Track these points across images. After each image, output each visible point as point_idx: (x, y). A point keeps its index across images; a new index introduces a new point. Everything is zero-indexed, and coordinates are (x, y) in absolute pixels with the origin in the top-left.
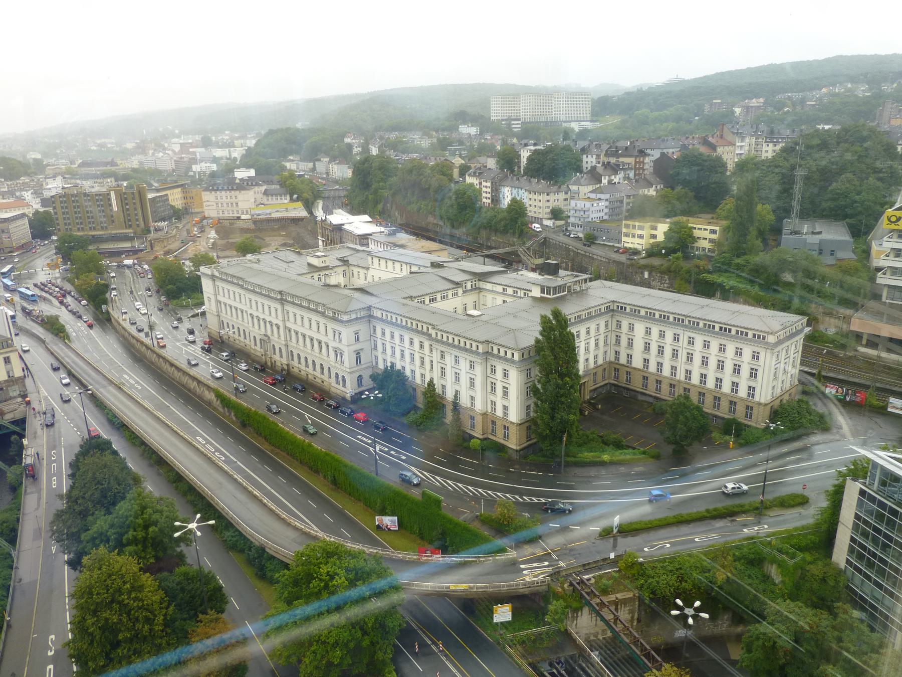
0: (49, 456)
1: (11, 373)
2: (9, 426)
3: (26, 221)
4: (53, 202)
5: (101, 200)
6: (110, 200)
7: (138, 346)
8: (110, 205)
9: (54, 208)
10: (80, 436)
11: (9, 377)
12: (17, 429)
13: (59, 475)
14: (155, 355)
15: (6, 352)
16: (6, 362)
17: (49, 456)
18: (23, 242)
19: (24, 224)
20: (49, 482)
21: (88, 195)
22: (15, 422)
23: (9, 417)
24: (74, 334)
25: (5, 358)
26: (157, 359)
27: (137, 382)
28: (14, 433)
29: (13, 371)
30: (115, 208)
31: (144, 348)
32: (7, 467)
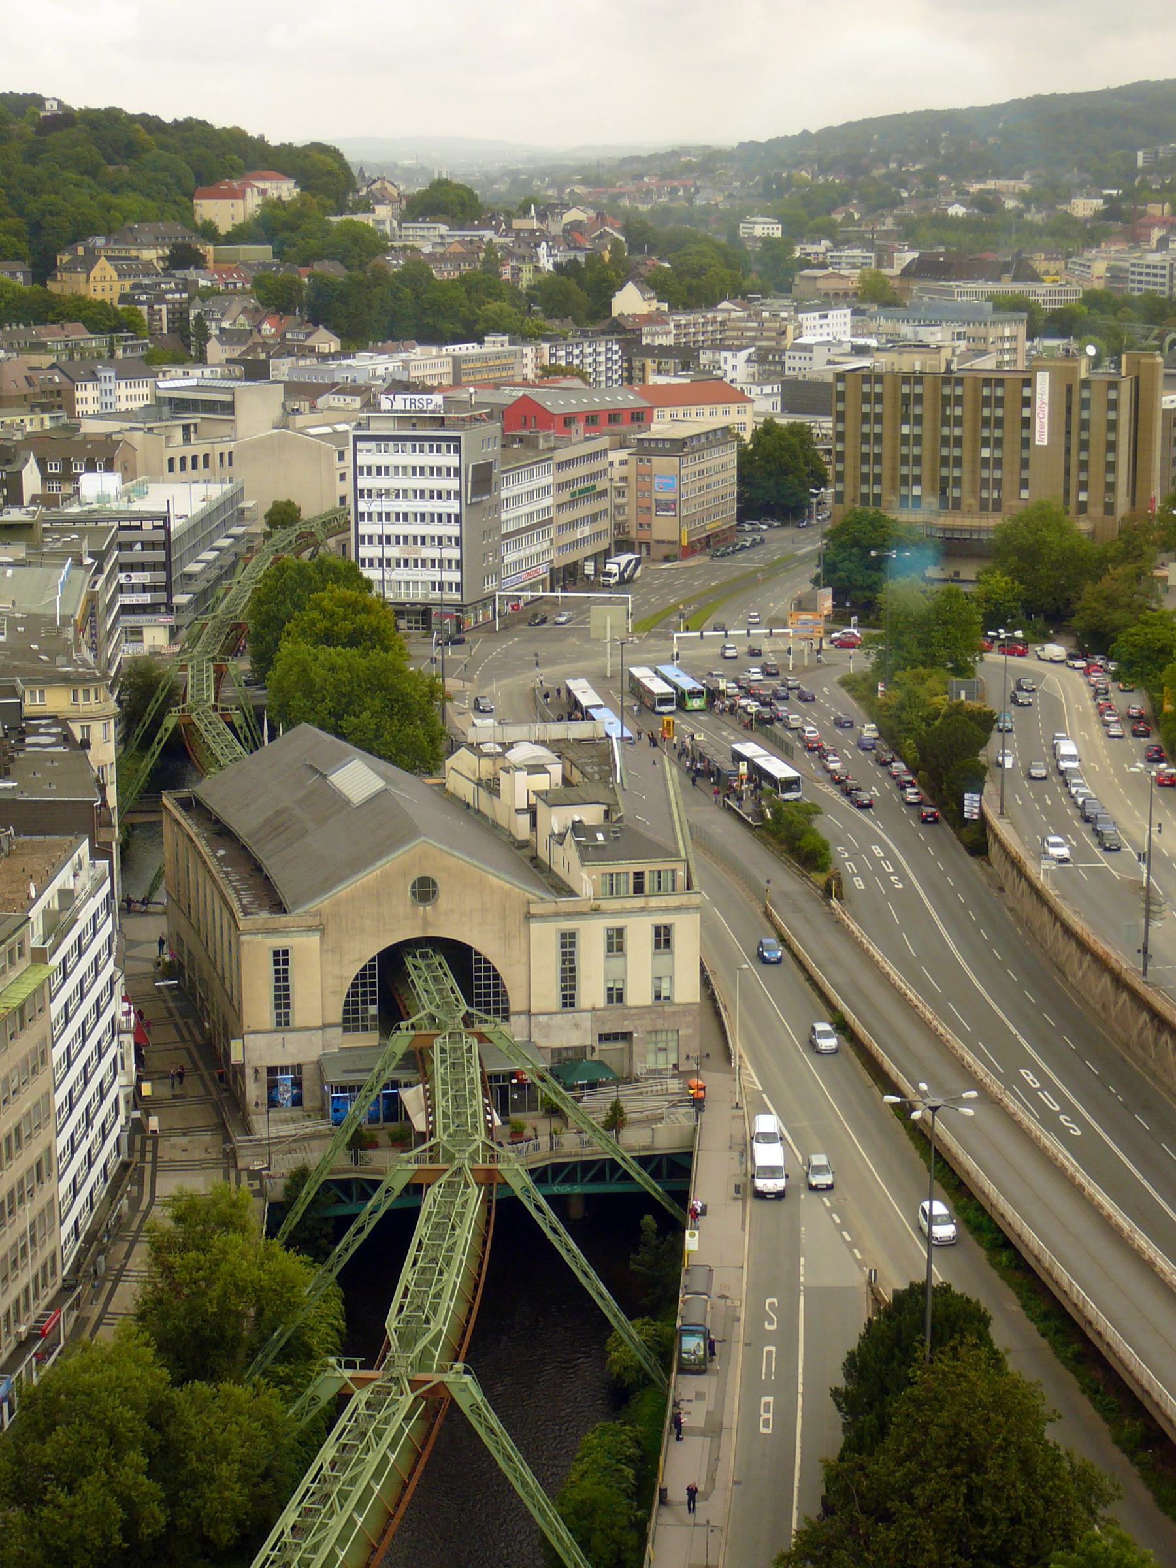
0: (758, 1316)
1: (665, 985)
2: (634, 1170)
3: (729, 457)
4: (841, 397)
5: (1000, 402)
6: (1028, 402)
7: (1079, 968)
8: (1027, 423)
9: (840, 417)
10: (860, 1264)
11: (658, 997)
12: (655, 1188)
13: (784, 1385)
14: (1145, 1016)
15: (667, 910)
16: (657, 945)
17: (758, 1316)
18: (712, 525)
19: (724, 467)
20: (751, 1414)
21: (959, 382)
22: (644, 1161)
23: (635, 1139)
24: (859, 883)
25: (657, 930)
26: (1149, 1034)
27: (1067, 1108)
28: (644, 1201)
29: (671, 978)
30: (1041, 436)
31: (1106, 979)
32: (623, 1317)
